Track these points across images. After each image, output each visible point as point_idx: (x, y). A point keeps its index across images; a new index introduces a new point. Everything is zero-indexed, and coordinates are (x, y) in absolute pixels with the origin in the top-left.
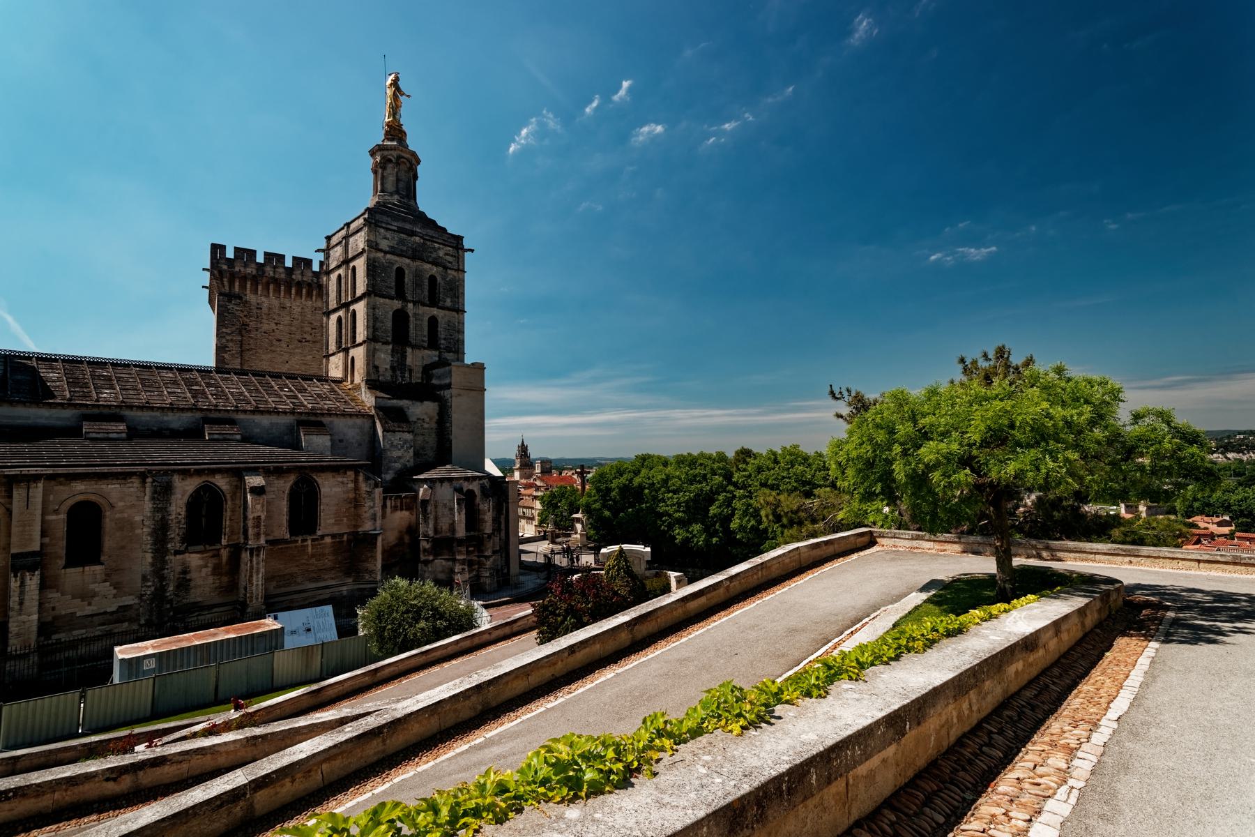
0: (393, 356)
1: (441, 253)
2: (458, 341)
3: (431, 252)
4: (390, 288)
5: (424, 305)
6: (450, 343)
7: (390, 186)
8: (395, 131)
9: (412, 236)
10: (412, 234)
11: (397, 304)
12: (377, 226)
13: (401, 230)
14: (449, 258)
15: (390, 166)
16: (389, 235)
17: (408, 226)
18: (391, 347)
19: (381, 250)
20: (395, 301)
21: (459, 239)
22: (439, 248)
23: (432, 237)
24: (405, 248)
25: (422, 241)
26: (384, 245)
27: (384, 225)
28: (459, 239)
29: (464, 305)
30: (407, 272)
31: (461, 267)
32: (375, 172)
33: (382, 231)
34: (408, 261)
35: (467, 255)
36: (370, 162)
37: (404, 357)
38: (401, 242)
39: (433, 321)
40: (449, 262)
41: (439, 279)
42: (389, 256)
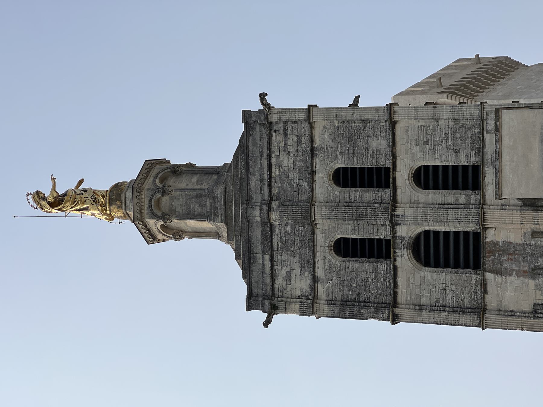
0: (508, 273)
1: (287, 161)
2: (456, 120)
3: (291, 184)
4: (375, 271)
5: (394, 202)
12: (273, 294)
14: (292, 140)
16: (281, 271)
17: (257, 233)
18: (489, 276)
19: (313, 288)
20: (398, 263)
22: (279, 165)
23: (262, 179)
24: (297, 240)
25: (274, 205)
27: (268, 280)
29: (377, 109)
34: (319, 236)
38: (287, 246)
40: (299, 142)
42: (320, 273)
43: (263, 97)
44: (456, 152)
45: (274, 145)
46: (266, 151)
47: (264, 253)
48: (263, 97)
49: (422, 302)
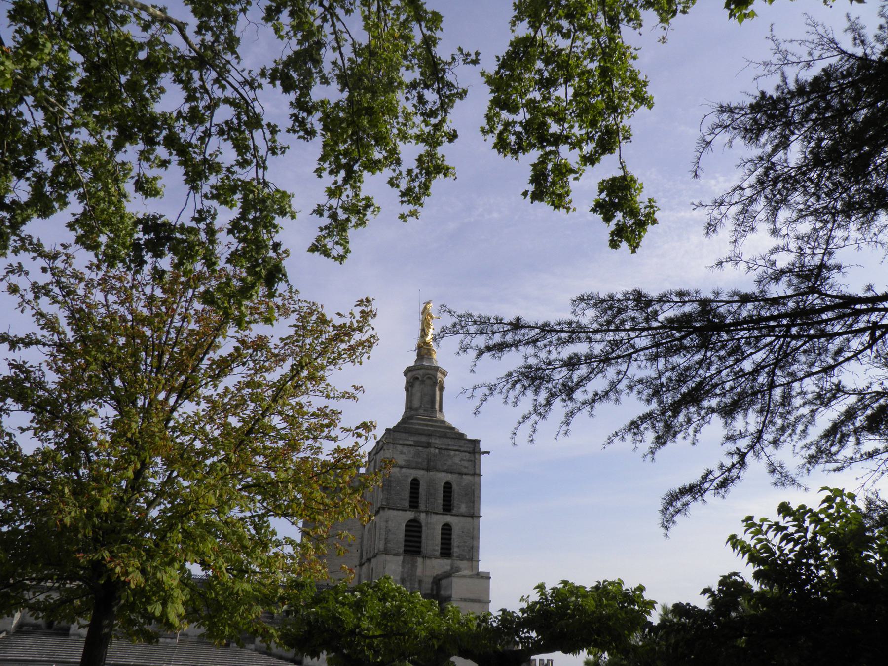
0: (403, 567)
1: (457, 460)
5: (437, 513)
6: (463, 550)
7: (416, 403)
8: (424, 351)
9: (427, 447)
10: (428, 445)
11: (410, 515)
13: (417, 444)
14: (466, 464)
15: (417, 383)
16: (405, 449)
17: (424, 439)
18: (401, 558)
20: (408, 513)
21: (476, 442)
22: (455, 455)
24: (420, 460)
25: (437, 451)
26: (401, 460)
27: (401, 442)
28: (476, 442)
30: (421, 483)
31: (477, 471)
32: (407, 389)
33: (399, 447)
34: (422, 472)
35: (484, 457)
36: (404, 380)
37: (414, 566)
39: (447, 530)
40: (465, 467)
41: (455, 487)
42: (404, 470)
43: (488, 453)
44: (458, 546)
45: (464, 454)
46: (462, 449)
47: (414, 441)
48: (488, 453)
49: (390, 523)
